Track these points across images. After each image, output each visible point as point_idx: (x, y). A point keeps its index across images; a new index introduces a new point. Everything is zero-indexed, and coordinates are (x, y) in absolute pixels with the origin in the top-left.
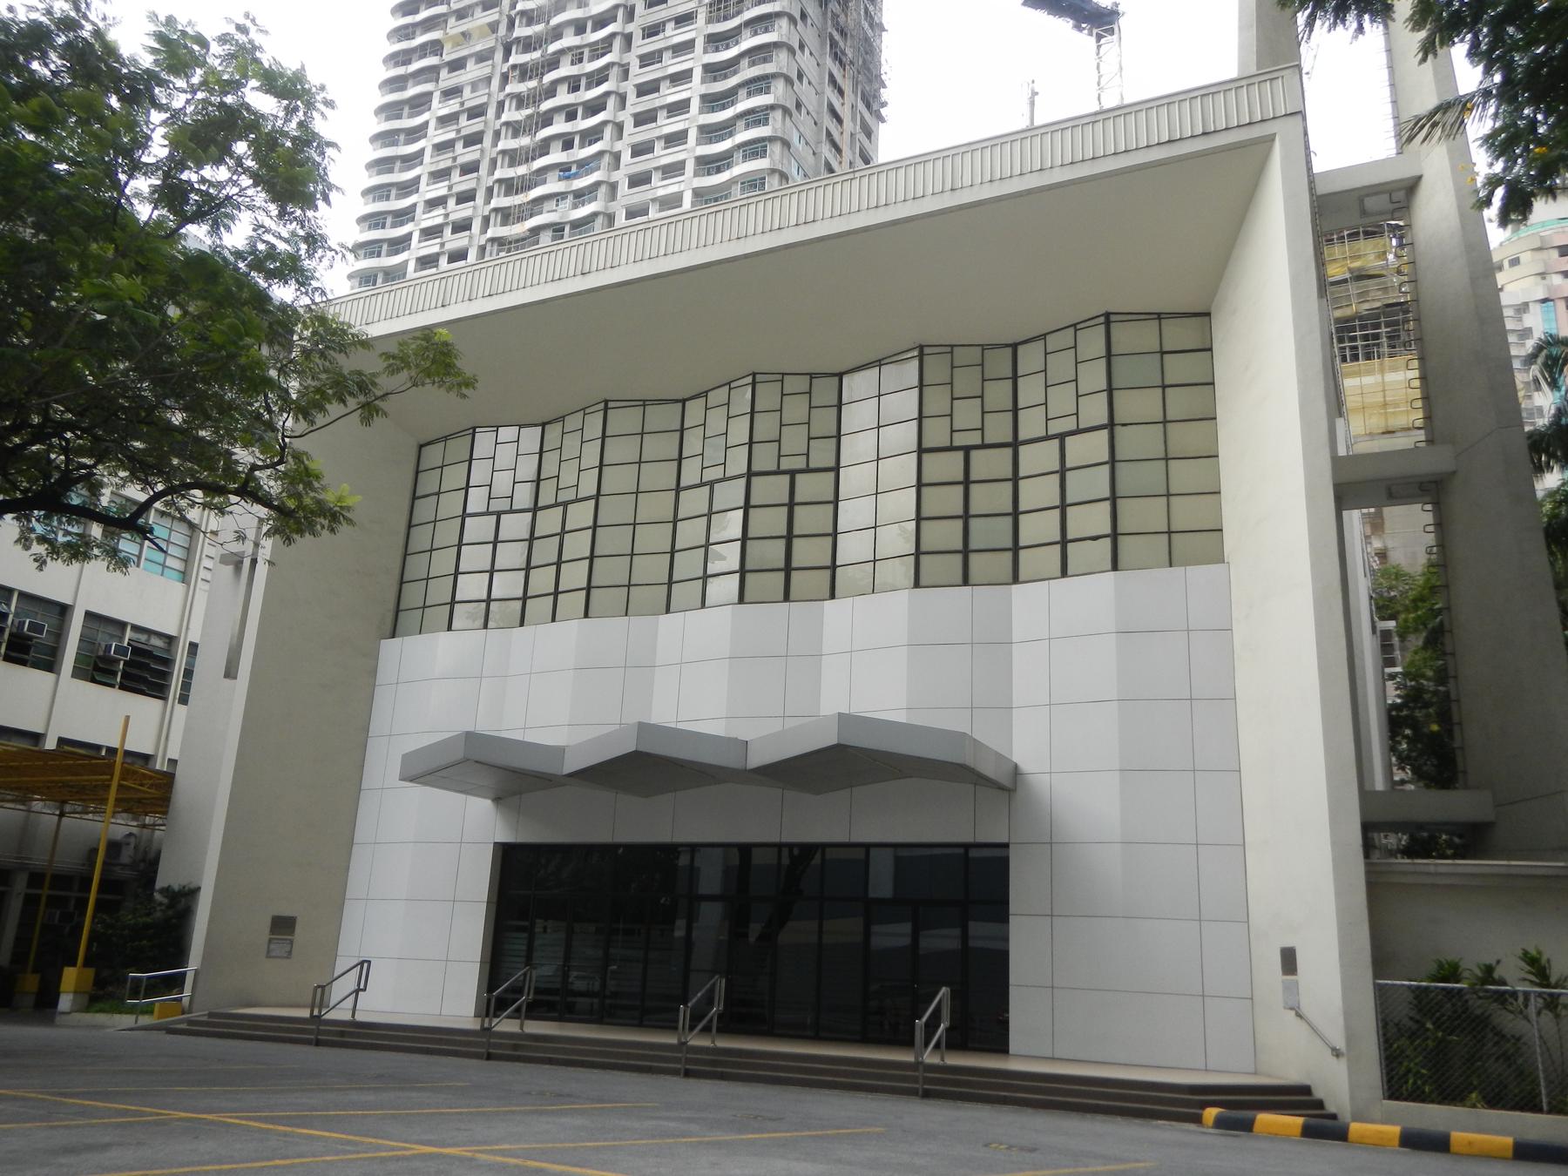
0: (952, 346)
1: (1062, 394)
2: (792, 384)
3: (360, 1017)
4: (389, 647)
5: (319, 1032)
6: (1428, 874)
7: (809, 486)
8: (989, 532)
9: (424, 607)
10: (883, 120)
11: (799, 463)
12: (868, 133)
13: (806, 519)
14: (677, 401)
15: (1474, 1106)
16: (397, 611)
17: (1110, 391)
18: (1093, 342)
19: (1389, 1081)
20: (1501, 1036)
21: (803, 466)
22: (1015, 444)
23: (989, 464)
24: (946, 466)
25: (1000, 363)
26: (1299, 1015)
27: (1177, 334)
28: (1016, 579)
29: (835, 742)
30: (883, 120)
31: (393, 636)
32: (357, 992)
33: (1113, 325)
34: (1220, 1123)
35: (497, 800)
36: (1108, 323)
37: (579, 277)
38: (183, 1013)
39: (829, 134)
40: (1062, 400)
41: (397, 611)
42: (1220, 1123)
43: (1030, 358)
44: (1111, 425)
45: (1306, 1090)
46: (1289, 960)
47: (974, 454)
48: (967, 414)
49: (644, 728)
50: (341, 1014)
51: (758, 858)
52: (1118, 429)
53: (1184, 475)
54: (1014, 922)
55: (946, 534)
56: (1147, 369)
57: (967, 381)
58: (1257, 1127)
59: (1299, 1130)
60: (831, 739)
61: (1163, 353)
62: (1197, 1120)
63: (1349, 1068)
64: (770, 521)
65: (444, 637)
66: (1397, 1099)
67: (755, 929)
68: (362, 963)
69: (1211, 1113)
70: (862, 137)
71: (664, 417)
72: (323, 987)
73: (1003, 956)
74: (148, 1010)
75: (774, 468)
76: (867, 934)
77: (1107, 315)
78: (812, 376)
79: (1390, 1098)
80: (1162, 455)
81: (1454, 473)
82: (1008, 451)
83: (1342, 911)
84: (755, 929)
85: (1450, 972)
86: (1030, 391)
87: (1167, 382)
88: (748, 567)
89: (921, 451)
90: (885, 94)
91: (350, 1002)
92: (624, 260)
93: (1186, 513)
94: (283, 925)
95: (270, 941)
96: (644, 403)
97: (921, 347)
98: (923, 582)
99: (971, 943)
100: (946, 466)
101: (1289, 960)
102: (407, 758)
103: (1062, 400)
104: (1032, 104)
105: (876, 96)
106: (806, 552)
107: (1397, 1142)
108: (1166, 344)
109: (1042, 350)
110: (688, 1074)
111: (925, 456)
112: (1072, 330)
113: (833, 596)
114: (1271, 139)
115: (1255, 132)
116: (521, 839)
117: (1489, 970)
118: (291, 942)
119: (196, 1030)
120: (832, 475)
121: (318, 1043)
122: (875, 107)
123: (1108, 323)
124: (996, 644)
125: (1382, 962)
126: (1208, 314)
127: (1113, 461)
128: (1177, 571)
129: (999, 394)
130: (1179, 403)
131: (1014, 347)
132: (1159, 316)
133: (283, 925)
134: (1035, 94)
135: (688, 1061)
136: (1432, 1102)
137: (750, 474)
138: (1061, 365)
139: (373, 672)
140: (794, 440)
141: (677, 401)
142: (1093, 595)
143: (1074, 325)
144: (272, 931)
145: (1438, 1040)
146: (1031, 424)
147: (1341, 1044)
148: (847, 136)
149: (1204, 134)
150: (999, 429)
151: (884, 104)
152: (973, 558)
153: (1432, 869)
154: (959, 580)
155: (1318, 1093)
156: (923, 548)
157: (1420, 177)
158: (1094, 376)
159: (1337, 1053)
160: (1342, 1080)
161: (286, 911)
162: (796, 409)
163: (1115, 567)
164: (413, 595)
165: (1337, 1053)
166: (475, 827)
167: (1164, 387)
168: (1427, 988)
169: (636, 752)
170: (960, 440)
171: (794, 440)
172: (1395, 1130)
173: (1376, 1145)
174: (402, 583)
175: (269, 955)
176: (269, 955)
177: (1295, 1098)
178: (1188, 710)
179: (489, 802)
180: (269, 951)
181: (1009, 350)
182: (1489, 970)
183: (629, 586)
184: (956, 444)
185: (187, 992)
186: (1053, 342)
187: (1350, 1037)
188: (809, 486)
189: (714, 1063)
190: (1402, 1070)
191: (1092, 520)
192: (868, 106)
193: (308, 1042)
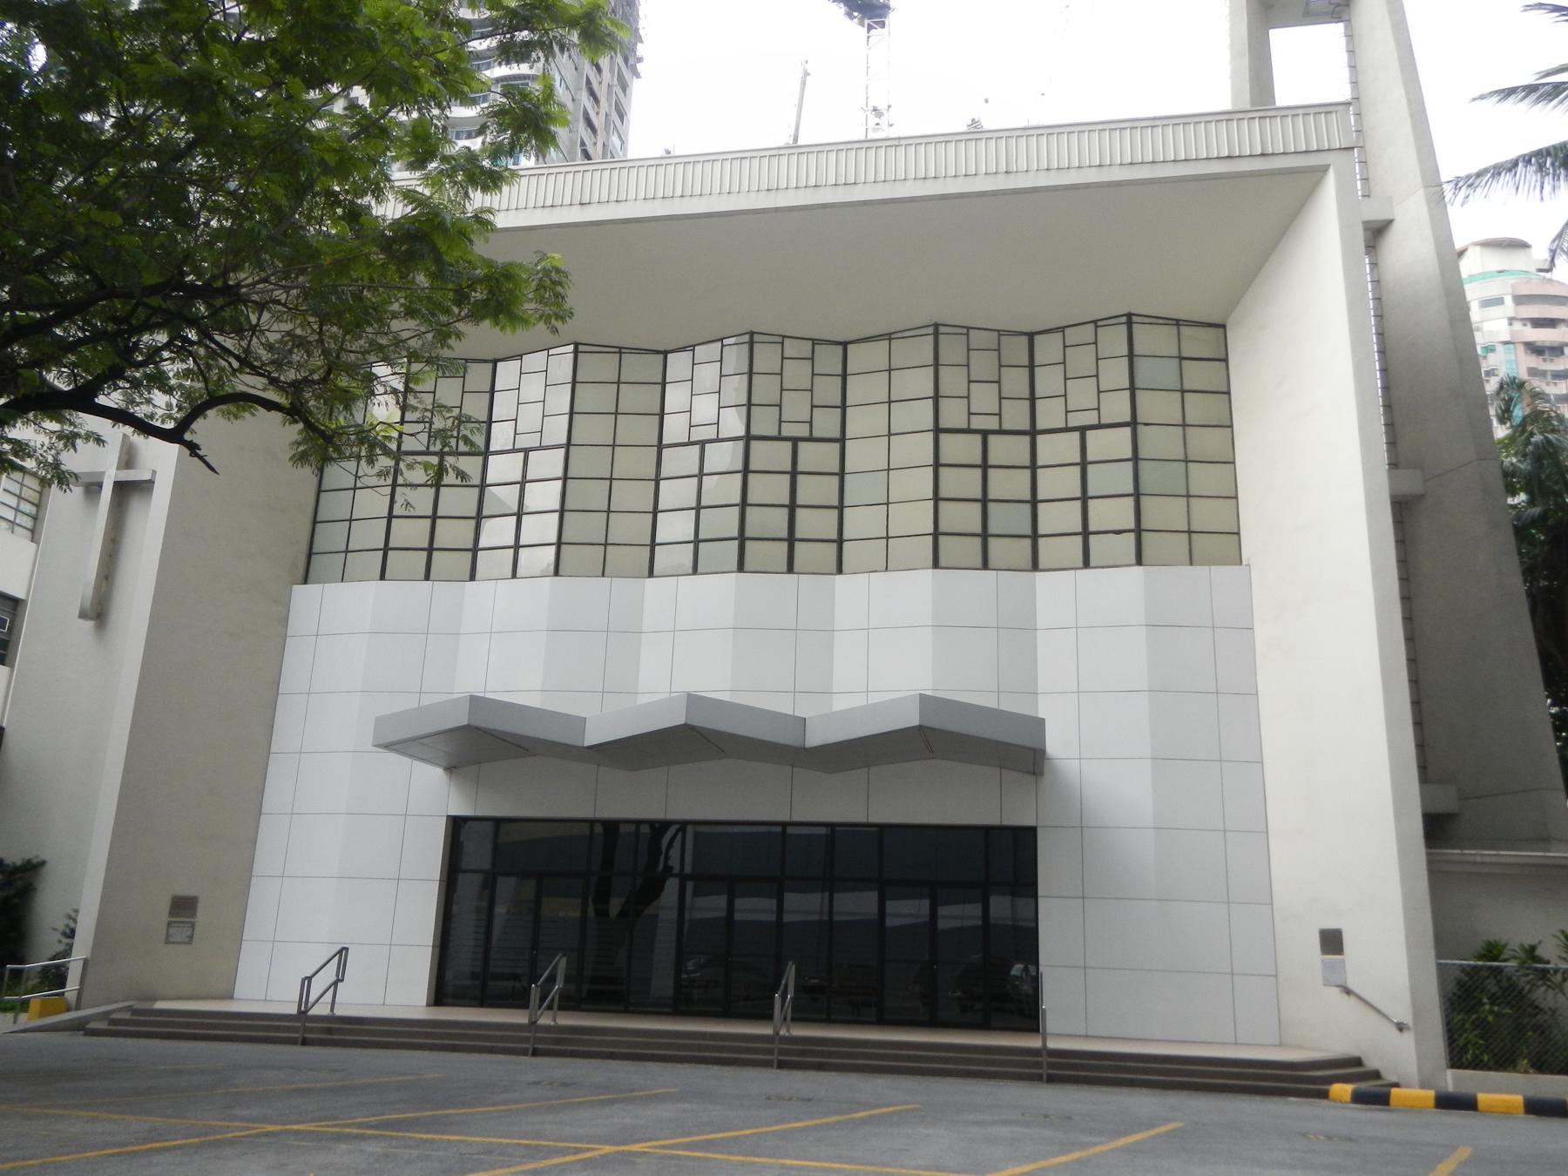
0: (968, 328)
1: (1081, 389)
2: (791, 348)
3: (339, 1012)
4: (305, 597)
5: (306, 1030)
6: (1475, 863)
7: (815, 456)
9: (347, 552)
10: (638, 76)
11: (803, 431)
12: (624, 87)
13: (810, 490)
14: (658, 352)
15: (1526, 1072)
16: (310, 554)
17: (1133, 389)
18: (1114, 341)
19: (1451, 1052)
20: (1537, 1009)
21: (807, 434)
22: (1033, 433)
23: (1006, 450)
24: (961, 448)
25: (1016, 350)
26: (1348, 992)
27: (1197, 342)
28: (1035, 566)
29: (915, 722)
30: (638, 76)
31: (305, 582)
32: (335, 984)
33: (1135, 326)
34: (1358, 1098)
35: (450, 769)
36: (1130, 324)
37: (576, 208)
38: (68, 1010)
39: (588, 82)
40: (1082, 393)
41: (310, 554)
42: (1358, 1098)
43: (1048, 348)
44: (1133, 424)
45: (1357, 1062)
46: (1332, 942)
47: (992, 439)
48: (985, 398)
49: (693, 700)
50: (321, 1010)
51: (623, 829)
52: (1140, 428)
53: (1203, 478)
54: (1043, 904)
56: (1166, 372)
57: (983, 365)
58: (1393, 1100)
59: (1432, 1102)
60: (913, 720)
61: (1181, 358)
62: (1324, 1095)
63: (1418, 1043)
64: (769, 489)
65: (375, 586)
66: (1459, 1067)
67: (615, 905)
68: (340, 952)
69: (1342, 1090)
70: (617, 89)
71: (636, 367)
72: (309, 979)
73: (1033, 933)
74: (24, 1006)
75: (775, 433)
76: (934, 914)
77: (1129, 316)
78: (815, 342)
79: (1452, 1067)
80: (1182, 457)
81: (1421, 497)
82: (1027, 439)
83: (1407, 896)
84: (615, 905)
85: (1492, 951)
86: (1048, 381)
87: (1186, 387)
88: (748, 533)
89: (938, 431)
90: (641, 50)
91: (328, 997)
92: (632, 196)
93: (1206, 514)
94: (183, 907)
95: (169, 924)
96: (620, 351)
97: (936, 326)
98: (942, 562)
99: (836, 918)
100: (961, 448)
101: (1332, 942)
102: (380, 722)
103: (1082, 393)
104: (804, 84)
105: (634, 51)
106: (807, 523)
107: (1522, 1109)
108: (1187, 351)
109: (1039, 344)
110: (781, 1065)
111: (943, 437)
112: (1092, 326)
113: (840, 571)
114: (1324, 169)
116: (480, 813)
117: (1533, 948)
118: (193, 925)
119: (117, 1028)
120: (837, 446)
121: (305, 1042)
122: (631, 61)
123: (1130, 324)
124: (1019, 630)
125: (1444, 942)
126: (1223, 326)
127: (1135, 458)
129: (1016, 381)
130: (1197, 408)
131: (1031, 336)
132: (1178, 323)
133: (183, 907)
134: (807, 74)
135: (781, 1052)
136: (1490, 1069)
137: (748, 438)
138: (1081, 360)
139: (284, 621)
140: (796, 407)
141: (658, 352)
142: (1119, 588)
143: (1095, 322)
144: (171, 914)
145: (1488, 1013)
146: (1049, 414)
147: (1407, 1019)
148: (605, 85)
149: (1263, 155)
150: (1016, 416)
151: (640, 60)
152: (992, 542)
153: (1478, 859)
154: (979, 564)
155: (1372, 1063)
156: (942, 528)
157: (1390, 222)
158: (1116, 374)
159: (1401, 1027)
160: (1407, 1051)
161: (187, 891)
162: (797, 373)
163: (1139, 562)
164: (331, 537)
165: (1401, 1027)
166: (432, 796)
167: (1183, 392)
168: (1480, 968)
169: (685, 725)
170: (977, 423)
171: (796, 407)
172: (1518, 1099)
173: (1506, 1113)
174: (315, 522)
175: (167, 942)
176: (167, 942)
177: (1350, 1067)
178: (1211, 704)
179: (437, 773)
180: (168, 936)
181: (1025, 339)
182: (1533, 948)
183: (606, 545)
184: (974, 426)
185: (72, 984)
186: (1072, 336)
187: (1417, 1012)
188: (810, 455)
189: (803, 1053)
190: (1461, 1042)
191: (1117, 513)
192: (626, 60)
193: (293, 1042)
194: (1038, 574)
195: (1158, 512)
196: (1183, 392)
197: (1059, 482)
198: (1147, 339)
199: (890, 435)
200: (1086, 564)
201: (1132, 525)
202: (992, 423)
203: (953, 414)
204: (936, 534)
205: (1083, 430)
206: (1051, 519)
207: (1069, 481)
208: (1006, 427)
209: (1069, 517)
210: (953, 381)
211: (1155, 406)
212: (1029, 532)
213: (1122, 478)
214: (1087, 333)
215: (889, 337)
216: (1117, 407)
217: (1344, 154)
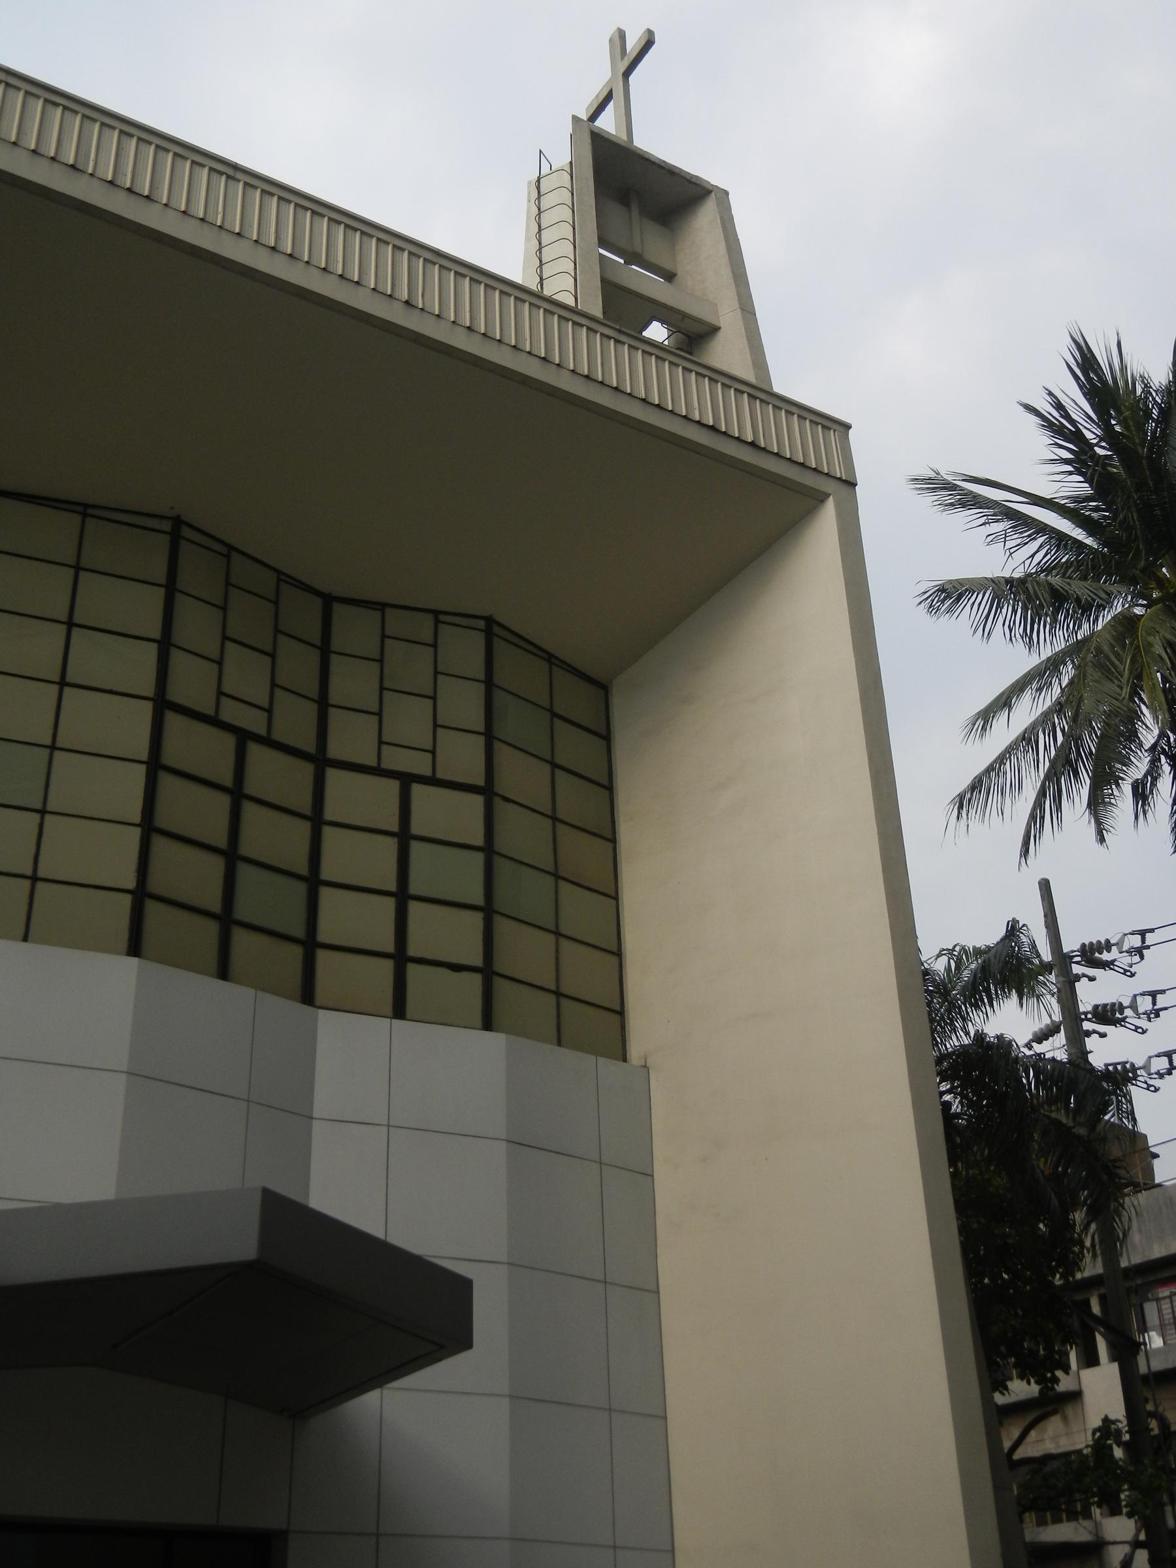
0: (231, 548)
8: (266, 899)
18: (464, 651)
22: (320, 761)
43: (354, 631)
48: (246, 675)
55: (191, 874)
86: (351, 682)
89: (162, 704)
93: (582, 972)
103: (409, 720)
114: (821, 498)
115: (809, 480)
126: (604, 688)
128: (567, 1057)
129: (299, 665)
131: (328, 601)
132: (550, 658)
138: (408, 665)
142: (457, 1067)
143: (436, 613)
146: (351, 738)
158: (464, 703)
163: (488, 1024)
167: (555, 766)
186: (396, 622)
194: (321, 1011)
195: (525, 951)
196: (555, 766)
197: (357, 857)
198: (515, 669)
199: (63, 683)
200: (399, 1011)
201: (478, 962)
202: (253, 721)
203: (191, 683)
204: (141, 895)
205: (407, 780)
206: (341, 917)
207: (375, 861)
208: (278, 735)
209: (370, 921)
210: (197, 627)
211: (520, 775)
212: (299, 932)
213: (464, 877)
214: (424, 627)
215: (84, 510)
216: (463, 757)
217: (844, 489)
